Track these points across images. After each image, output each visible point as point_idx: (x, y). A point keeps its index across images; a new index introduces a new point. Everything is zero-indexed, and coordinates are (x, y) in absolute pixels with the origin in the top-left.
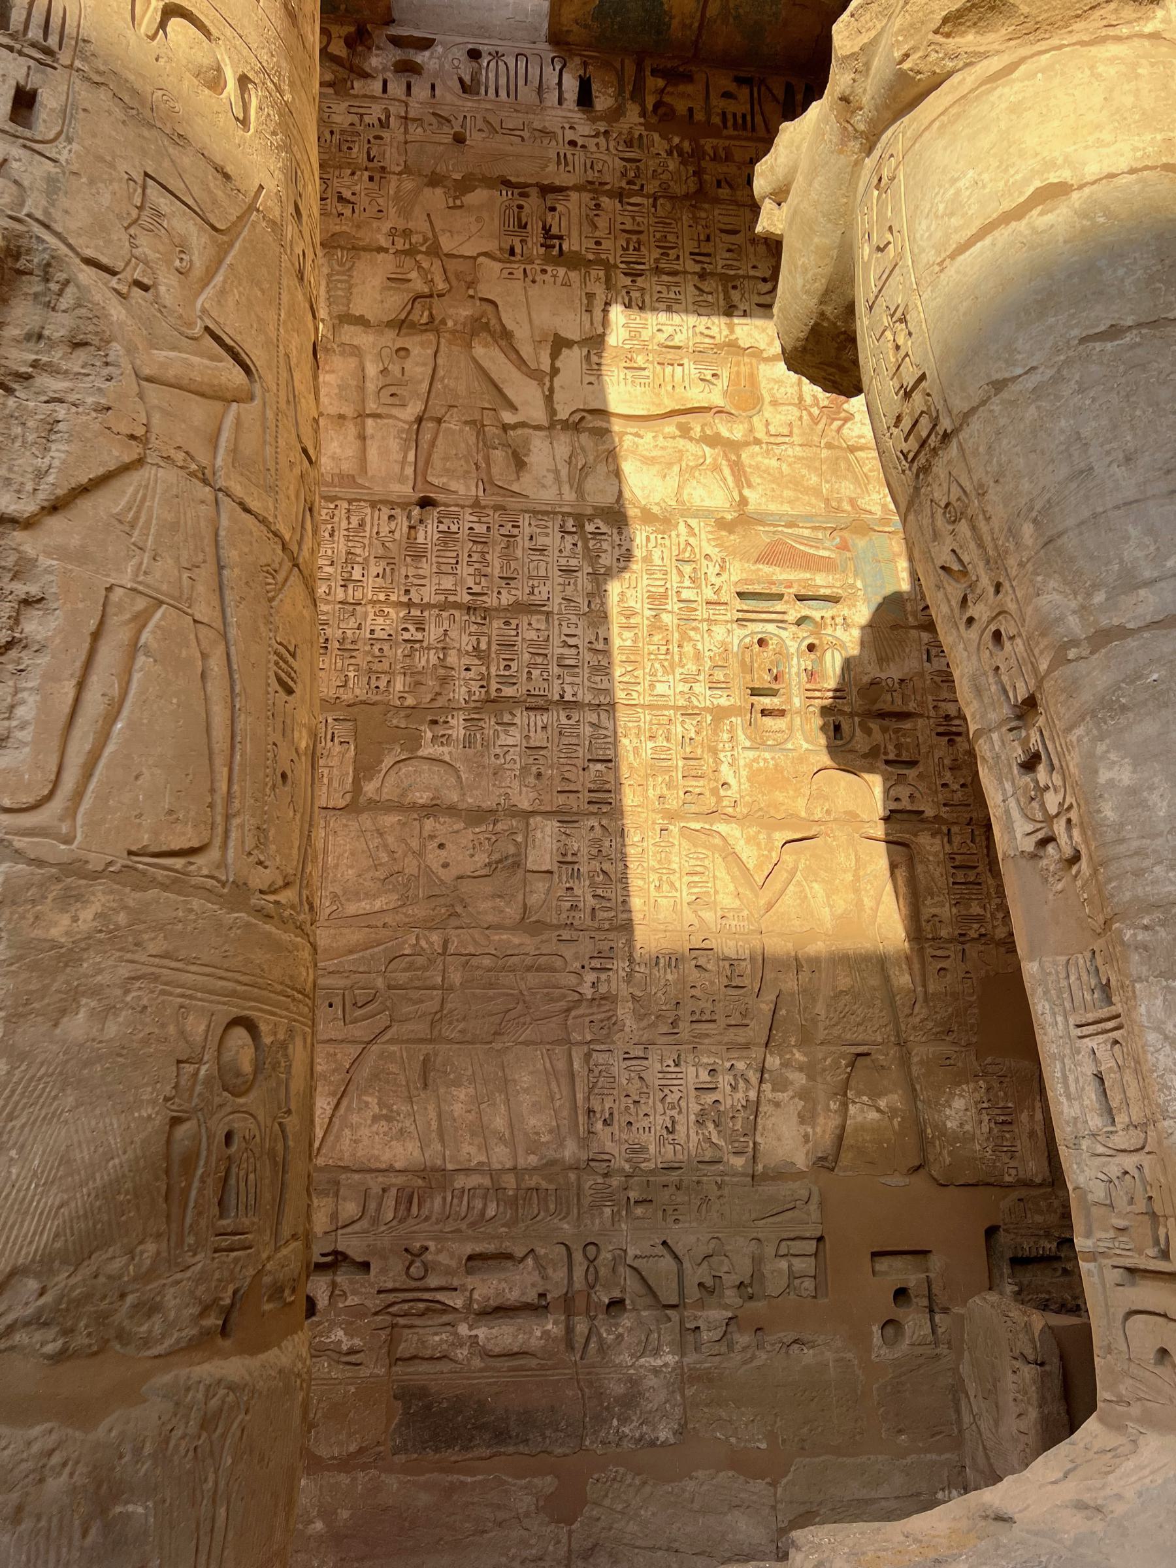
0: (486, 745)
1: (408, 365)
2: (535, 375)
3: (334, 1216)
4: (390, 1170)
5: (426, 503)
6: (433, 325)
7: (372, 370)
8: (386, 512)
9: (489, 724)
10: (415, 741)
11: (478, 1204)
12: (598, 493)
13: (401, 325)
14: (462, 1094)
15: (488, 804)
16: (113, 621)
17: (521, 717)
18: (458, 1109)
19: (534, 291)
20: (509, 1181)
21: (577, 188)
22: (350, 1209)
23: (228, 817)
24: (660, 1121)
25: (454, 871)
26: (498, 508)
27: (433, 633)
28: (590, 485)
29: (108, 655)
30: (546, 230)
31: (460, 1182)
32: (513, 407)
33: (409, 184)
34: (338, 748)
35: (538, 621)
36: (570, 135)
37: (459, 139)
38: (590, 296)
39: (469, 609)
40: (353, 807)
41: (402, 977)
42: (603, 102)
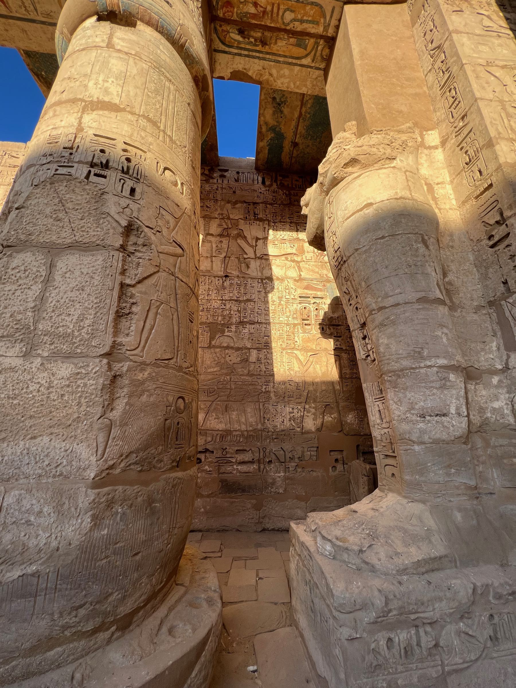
0: (240, 332)
1: (222, 244)
2: (252, 246)
3: (206, 441)
4: (218, 430)
5: (226, 276)
6: (228, 235)
7: (214, 246)
8: (217, 278)
9: (241, 327)
10: (224, 332)
11: (238, 438)
12: (266, 273)
13: (221, 235)
14: (235, 413)
15: (240, 346)
16: (152, 307)
17: (248, 326)
18: (234, 417)
19: (251, 227)
20: (246, 433)
21: (262, 203)
22: (209, 439)
23: (178, 351)
24: (281, 420)
25: (232, 362)
27: (228, 306)
28: (264, 272)
29: (151, 315)
30: (255, 214)
31: (234, 433)
33: (223, 203)
34: (206, 333)
36: (260, 191)
37: (234, 192)
38: (265, 228)
39: (236, 301)
40: (209, 347)
41: (221, 386)
42: (268, 183)
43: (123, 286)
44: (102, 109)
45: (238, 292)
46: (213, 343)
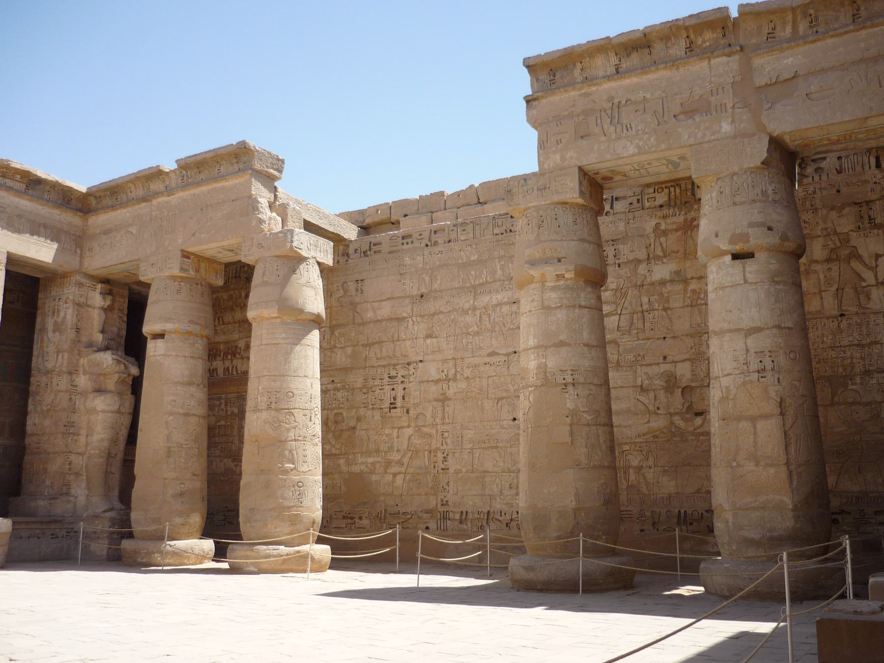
2: (870, 268)
5: (842, 315)
6: (838, 259)
7: (822, 277)
9: (867, 378)
13: (828, 260)
17: (876, 375)
21: (878, 199)
26: (864, 313)
27: (849, 354)
30: (869, 217)
32: (864, 280)
33: (825, 212)
35: (878, 346)
36: (874, 180)
37: (838, 191)
39: (858, 345)
40: (832, 404)
43: (785, 433)
44: (754, 333)
45: (860, 334)
46: (836, 399)
